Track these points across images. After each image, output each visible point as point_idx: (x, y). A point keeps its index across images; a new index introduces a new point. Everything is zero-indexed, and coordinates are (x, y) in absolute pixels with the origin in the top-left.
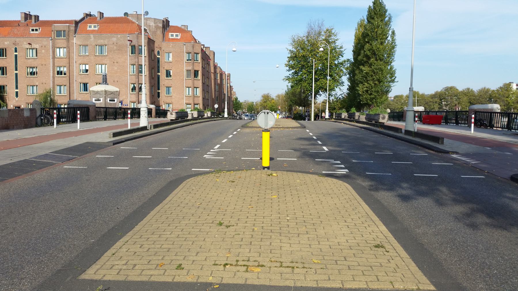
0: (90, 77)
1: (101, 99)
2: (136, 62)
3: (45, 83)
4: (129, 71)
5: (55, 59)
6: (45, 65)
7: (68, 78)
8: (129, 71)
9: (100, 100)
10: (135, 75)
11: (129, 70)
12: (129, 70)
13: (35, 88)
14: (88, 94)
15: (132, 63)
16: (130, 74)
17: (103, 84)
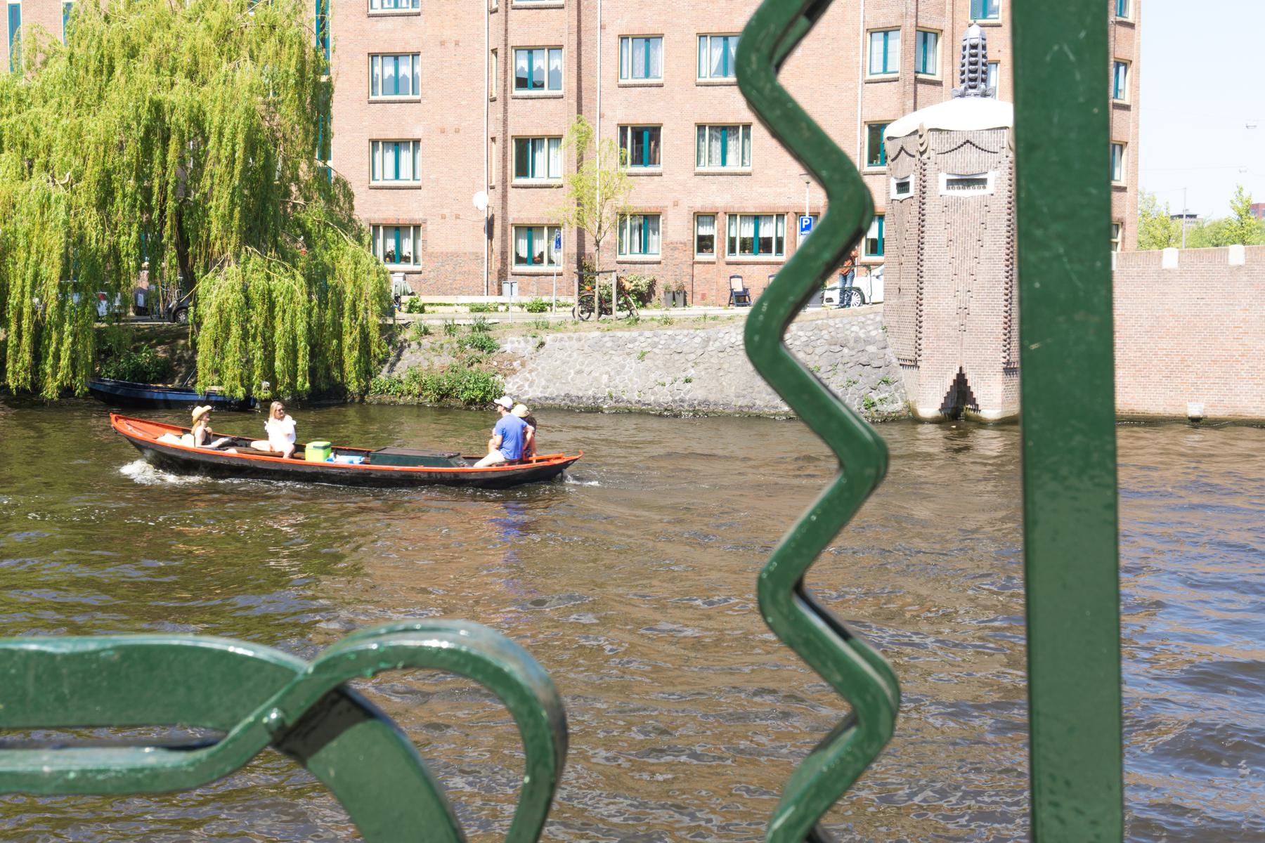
0: (673, 98)
1: (991, 177)
2: (903, 16)
3: (457, 131)
4: (864, 62)
5: (512, 13)
6: (457, 44)
7: (571, 101)
8: (864, 62)
9: (982, 182)
10: (896, 80)
11: (864, 55)
12: (864, 55)
13: (406, 156)
14: (656, 178)
15: (882, 23)
16: (868, 77)
17: (976, 95)
